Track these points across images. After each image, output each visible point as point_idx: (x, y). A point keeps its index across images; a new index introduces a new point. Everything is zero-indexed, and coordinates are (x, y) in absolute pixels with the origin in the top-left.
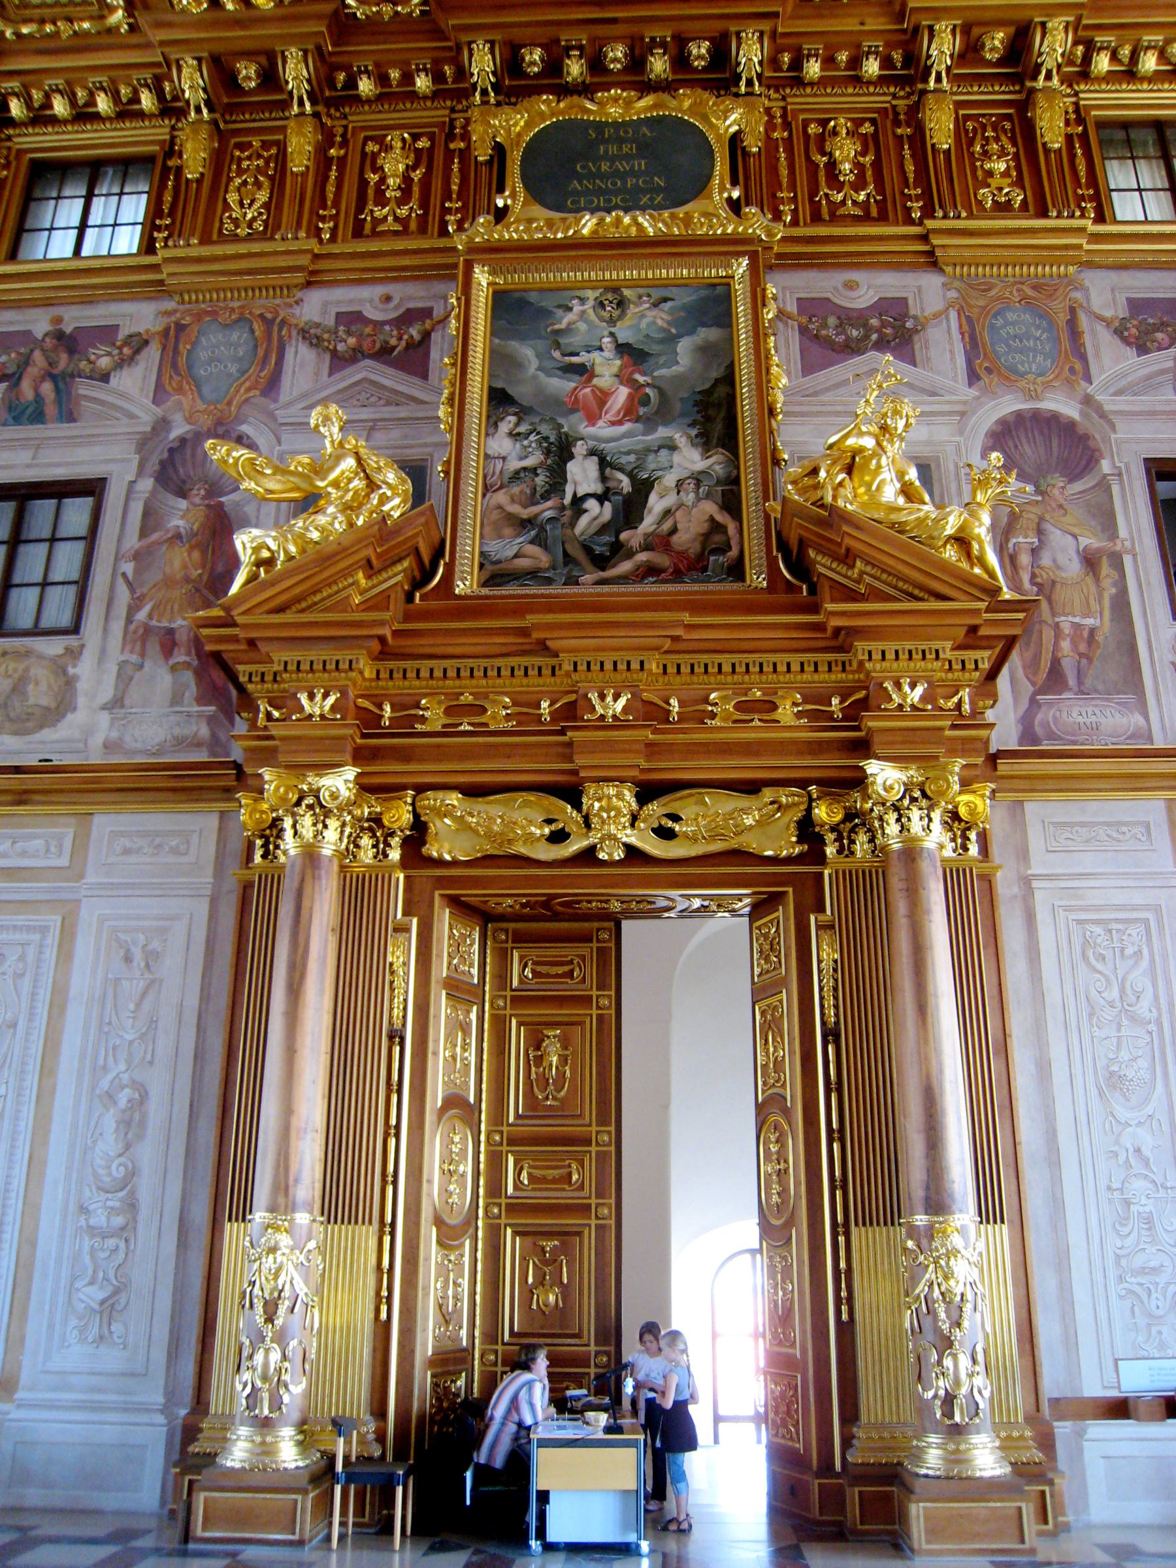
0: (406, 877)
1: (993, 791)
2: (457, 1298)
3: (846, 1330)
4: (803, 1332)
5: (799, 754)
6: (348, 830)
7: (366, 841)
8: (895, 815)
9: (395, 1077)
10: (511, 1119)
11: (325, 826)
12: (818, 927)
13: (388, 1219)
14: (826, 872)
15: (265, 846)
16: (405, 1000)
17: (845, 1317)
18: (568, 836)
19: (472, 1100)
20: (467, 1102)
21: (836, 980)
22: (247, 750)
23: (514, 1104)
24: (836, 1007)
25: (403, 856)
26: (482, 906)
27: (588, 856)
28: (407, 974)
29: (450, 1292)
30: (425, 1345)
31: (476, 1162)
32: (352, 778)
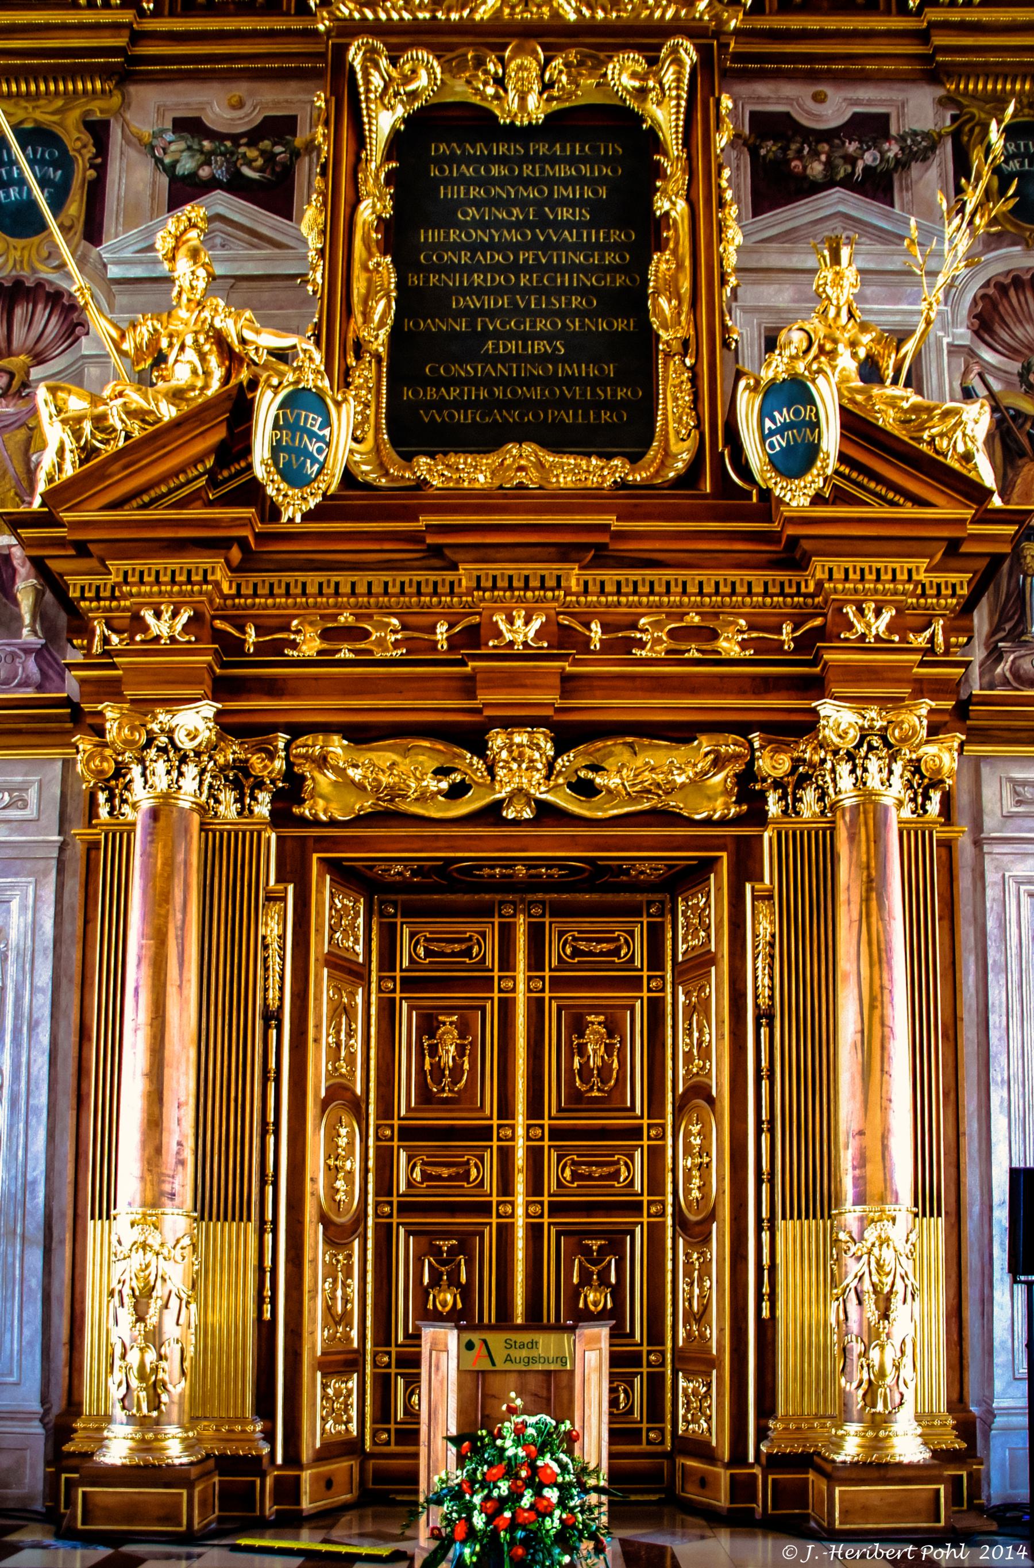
0: (278, 838)
1: (962, 744)
2: (346, 1301)
3: (767, 1329)
4: (721, 1330)
5: (742, 693)
6: (208, 778)
7: (228, 796)
8: (849, 766)
9: (272, 1065)
10: (403, 1113)
11: (181, 774)
12: (754, 898)
13: (269, 1216)
14: (766, 835)
15: (110, 800)
16: (282, 978)
17: (766, 1314)
18: (469, 788)
19: (358, 1091)
20: (354, 1093)
21: (772, 957)
22: (83, 681)
23: (404, 1099)
24: (772, 989)
25: (271, 812)
26: (368, 873)
27: (491, 814)
28: (283, 948)
29: (339, 1293)
30: (313, 1348)
31: (365, 1158)
32: (211, 715)
